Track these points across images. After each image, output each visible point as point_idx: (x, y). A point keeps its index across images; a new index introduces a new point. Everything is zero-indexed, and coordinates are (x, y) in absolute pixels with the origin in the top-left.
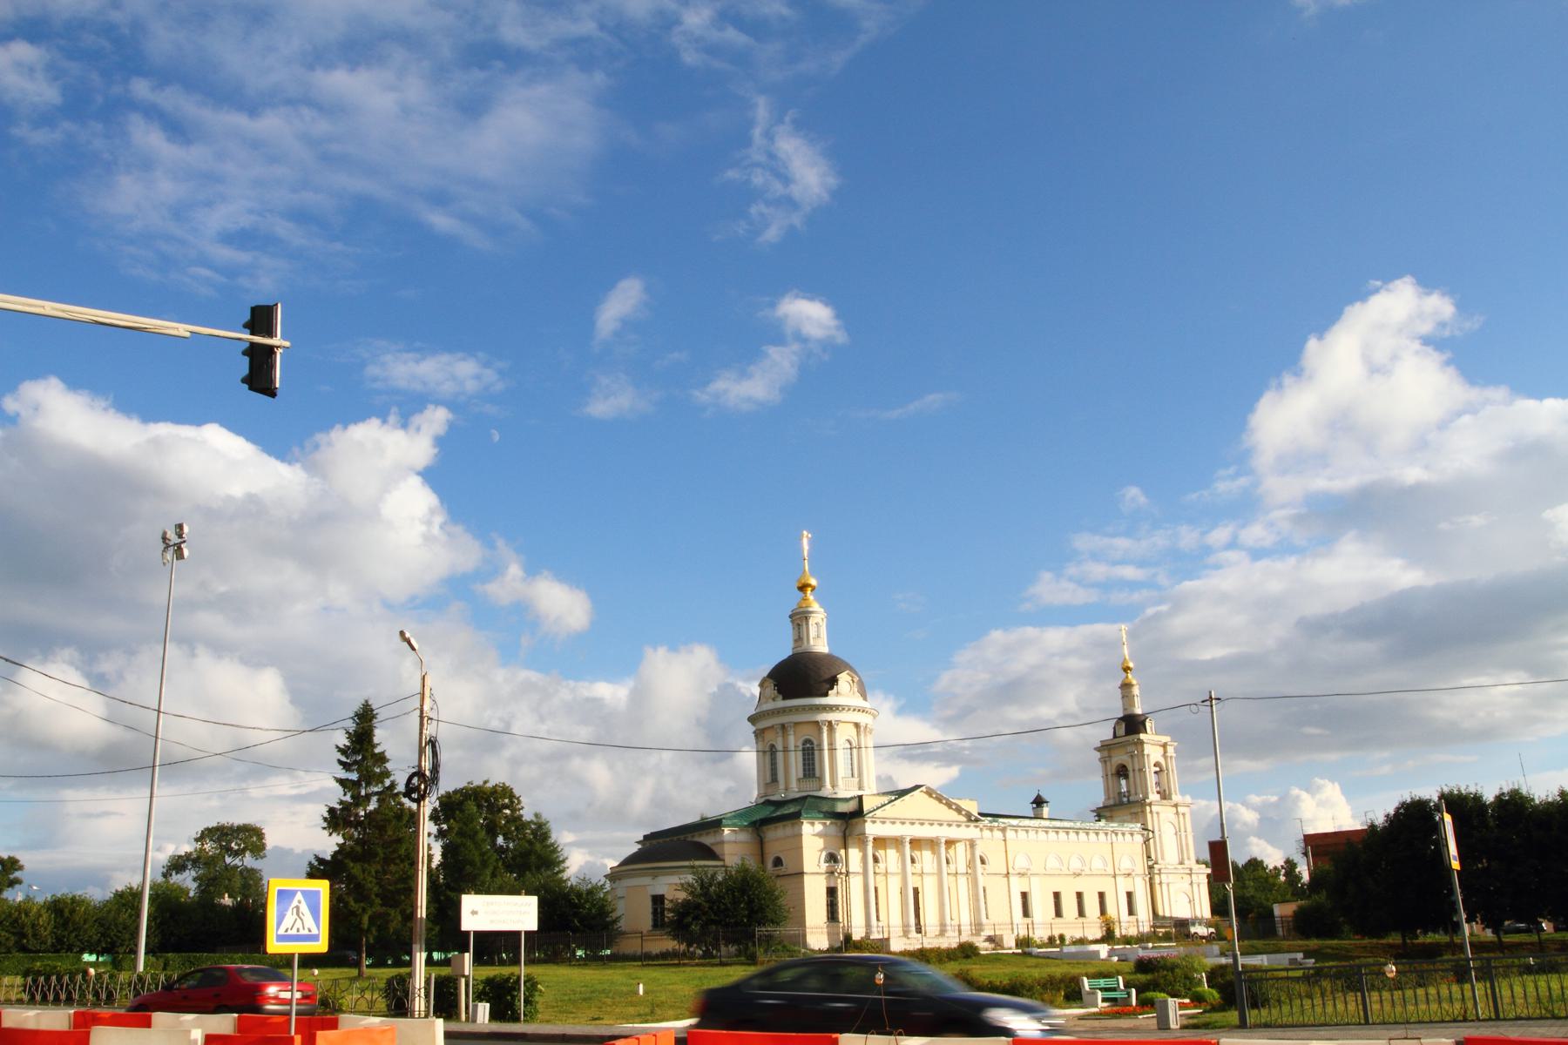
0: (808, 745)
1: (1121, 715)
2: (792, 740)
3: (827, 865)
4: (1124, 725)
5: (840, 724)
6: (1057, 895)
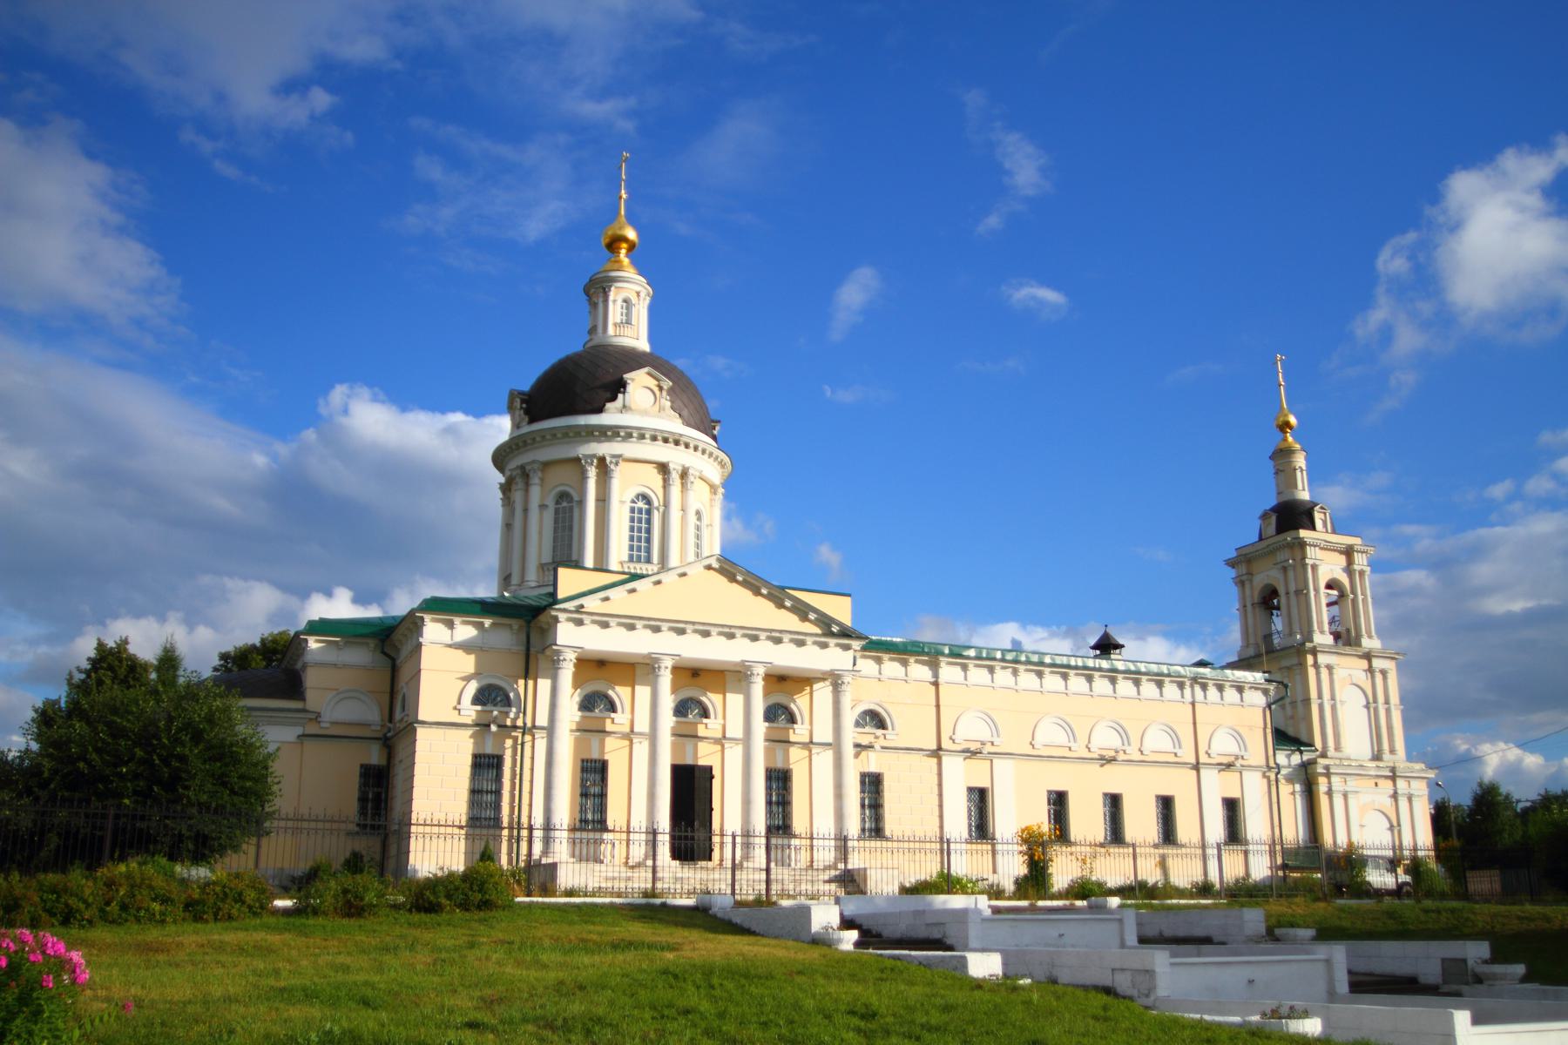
0: (565, 504)
2: (535, 492)
3: (479, 708)
5: (622, 464)
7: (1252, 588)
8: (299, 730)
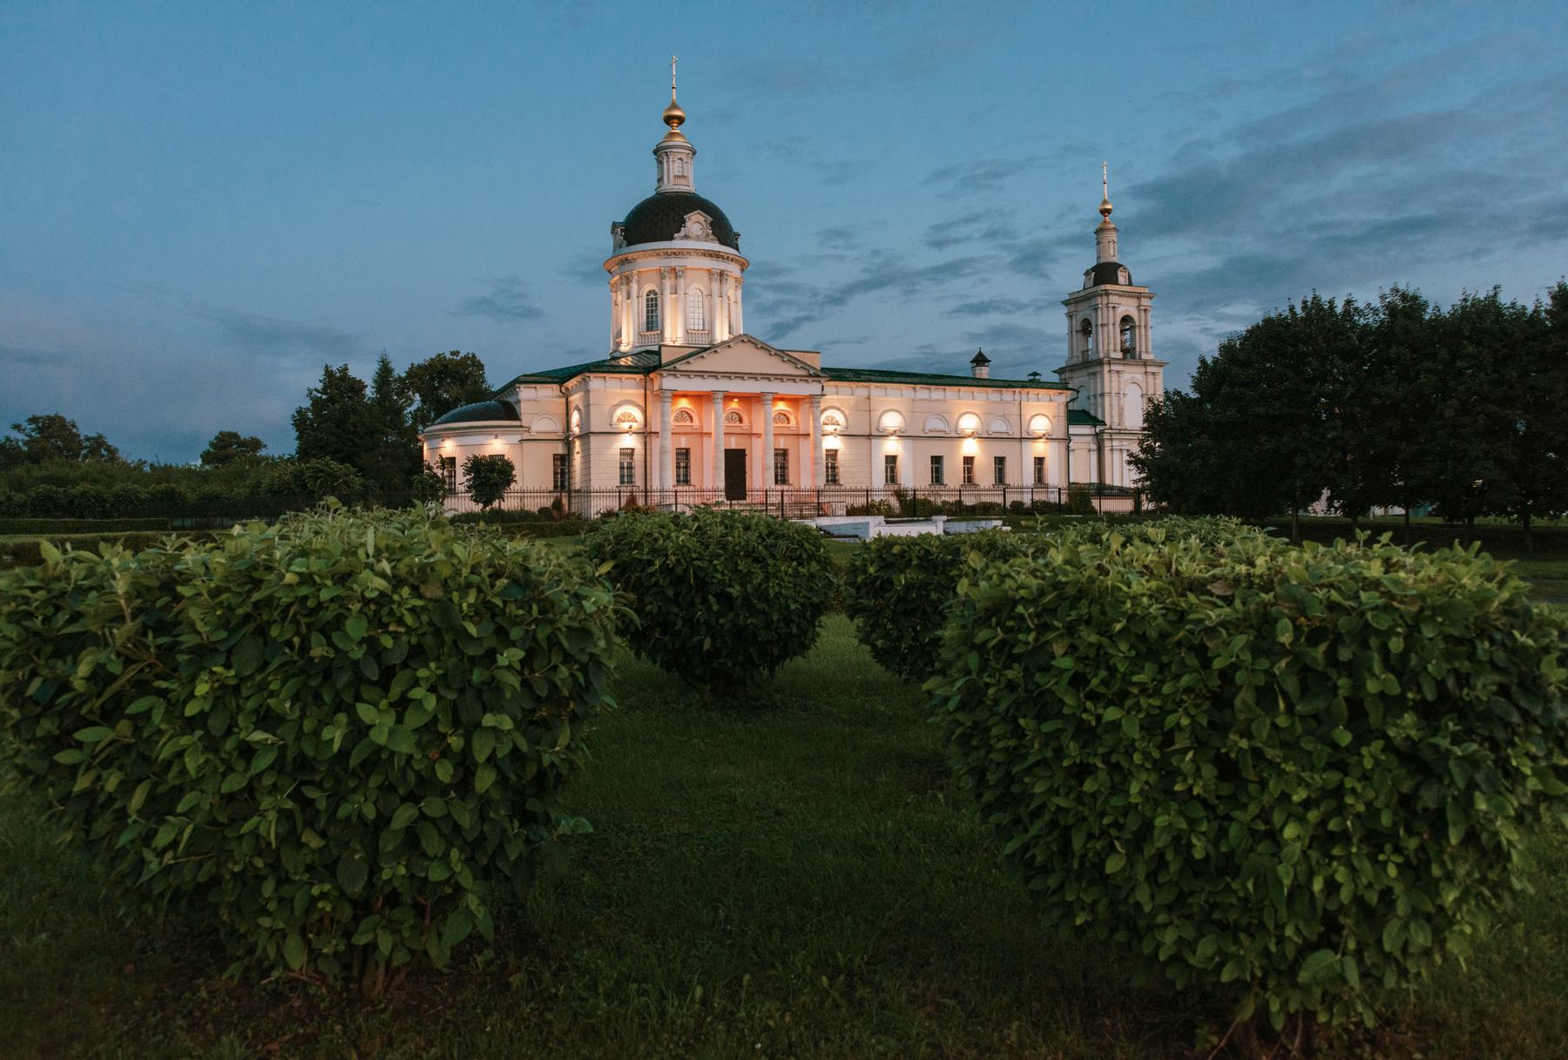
5: (688, 272)
6: (937, 461)
8: (519, 438)
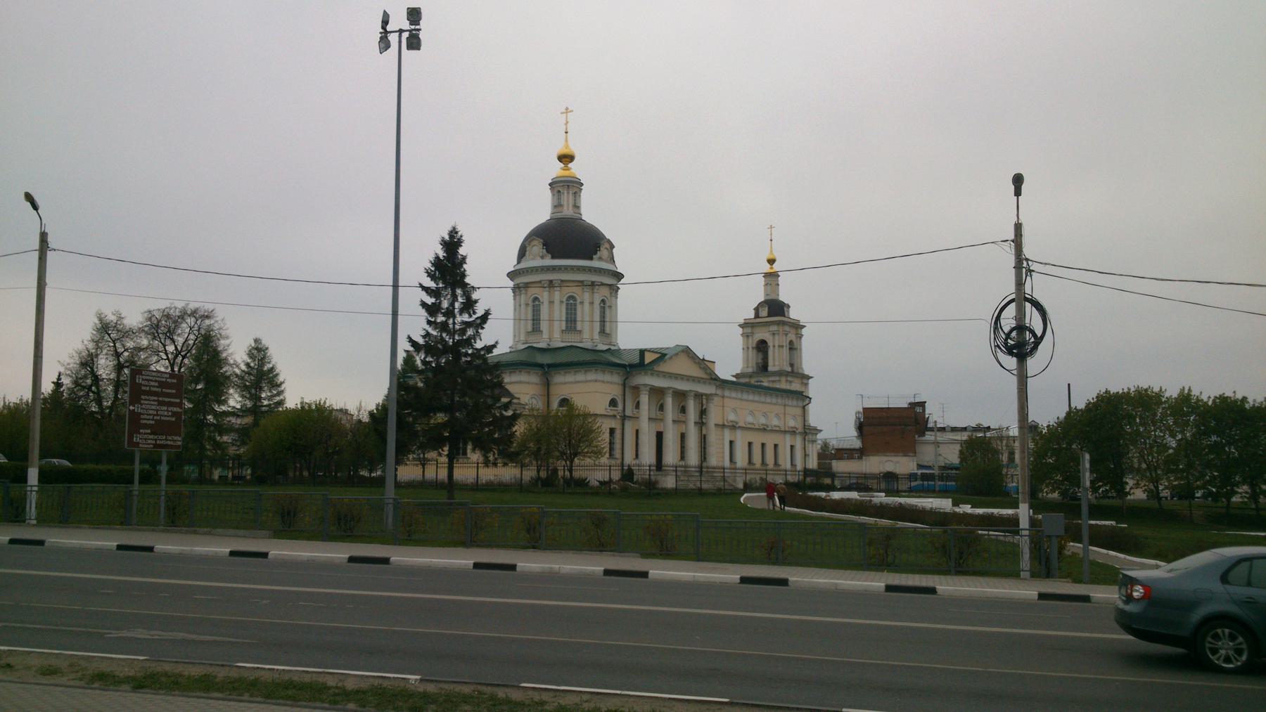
0: (571, 302)
1: (763, 300)
2: (557, 294)
4: (767, 309)
7: (752, 340)
